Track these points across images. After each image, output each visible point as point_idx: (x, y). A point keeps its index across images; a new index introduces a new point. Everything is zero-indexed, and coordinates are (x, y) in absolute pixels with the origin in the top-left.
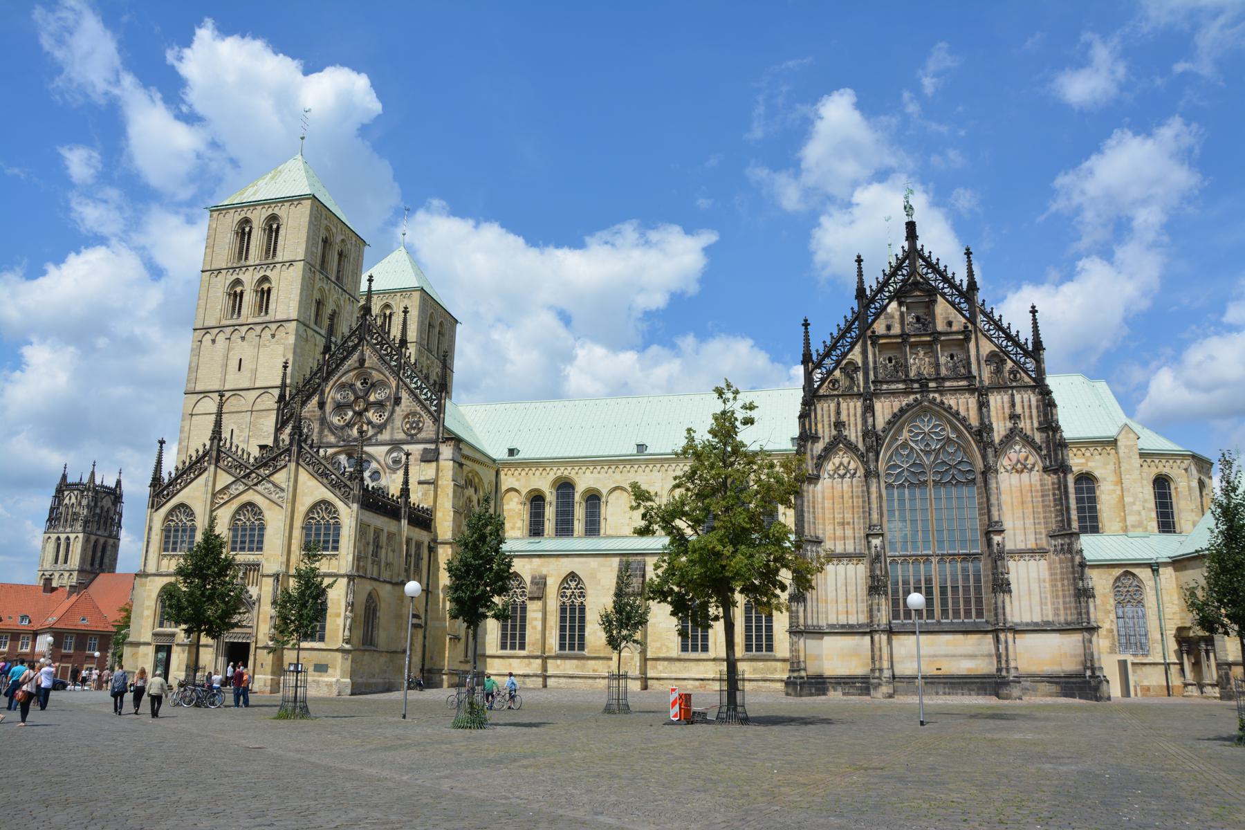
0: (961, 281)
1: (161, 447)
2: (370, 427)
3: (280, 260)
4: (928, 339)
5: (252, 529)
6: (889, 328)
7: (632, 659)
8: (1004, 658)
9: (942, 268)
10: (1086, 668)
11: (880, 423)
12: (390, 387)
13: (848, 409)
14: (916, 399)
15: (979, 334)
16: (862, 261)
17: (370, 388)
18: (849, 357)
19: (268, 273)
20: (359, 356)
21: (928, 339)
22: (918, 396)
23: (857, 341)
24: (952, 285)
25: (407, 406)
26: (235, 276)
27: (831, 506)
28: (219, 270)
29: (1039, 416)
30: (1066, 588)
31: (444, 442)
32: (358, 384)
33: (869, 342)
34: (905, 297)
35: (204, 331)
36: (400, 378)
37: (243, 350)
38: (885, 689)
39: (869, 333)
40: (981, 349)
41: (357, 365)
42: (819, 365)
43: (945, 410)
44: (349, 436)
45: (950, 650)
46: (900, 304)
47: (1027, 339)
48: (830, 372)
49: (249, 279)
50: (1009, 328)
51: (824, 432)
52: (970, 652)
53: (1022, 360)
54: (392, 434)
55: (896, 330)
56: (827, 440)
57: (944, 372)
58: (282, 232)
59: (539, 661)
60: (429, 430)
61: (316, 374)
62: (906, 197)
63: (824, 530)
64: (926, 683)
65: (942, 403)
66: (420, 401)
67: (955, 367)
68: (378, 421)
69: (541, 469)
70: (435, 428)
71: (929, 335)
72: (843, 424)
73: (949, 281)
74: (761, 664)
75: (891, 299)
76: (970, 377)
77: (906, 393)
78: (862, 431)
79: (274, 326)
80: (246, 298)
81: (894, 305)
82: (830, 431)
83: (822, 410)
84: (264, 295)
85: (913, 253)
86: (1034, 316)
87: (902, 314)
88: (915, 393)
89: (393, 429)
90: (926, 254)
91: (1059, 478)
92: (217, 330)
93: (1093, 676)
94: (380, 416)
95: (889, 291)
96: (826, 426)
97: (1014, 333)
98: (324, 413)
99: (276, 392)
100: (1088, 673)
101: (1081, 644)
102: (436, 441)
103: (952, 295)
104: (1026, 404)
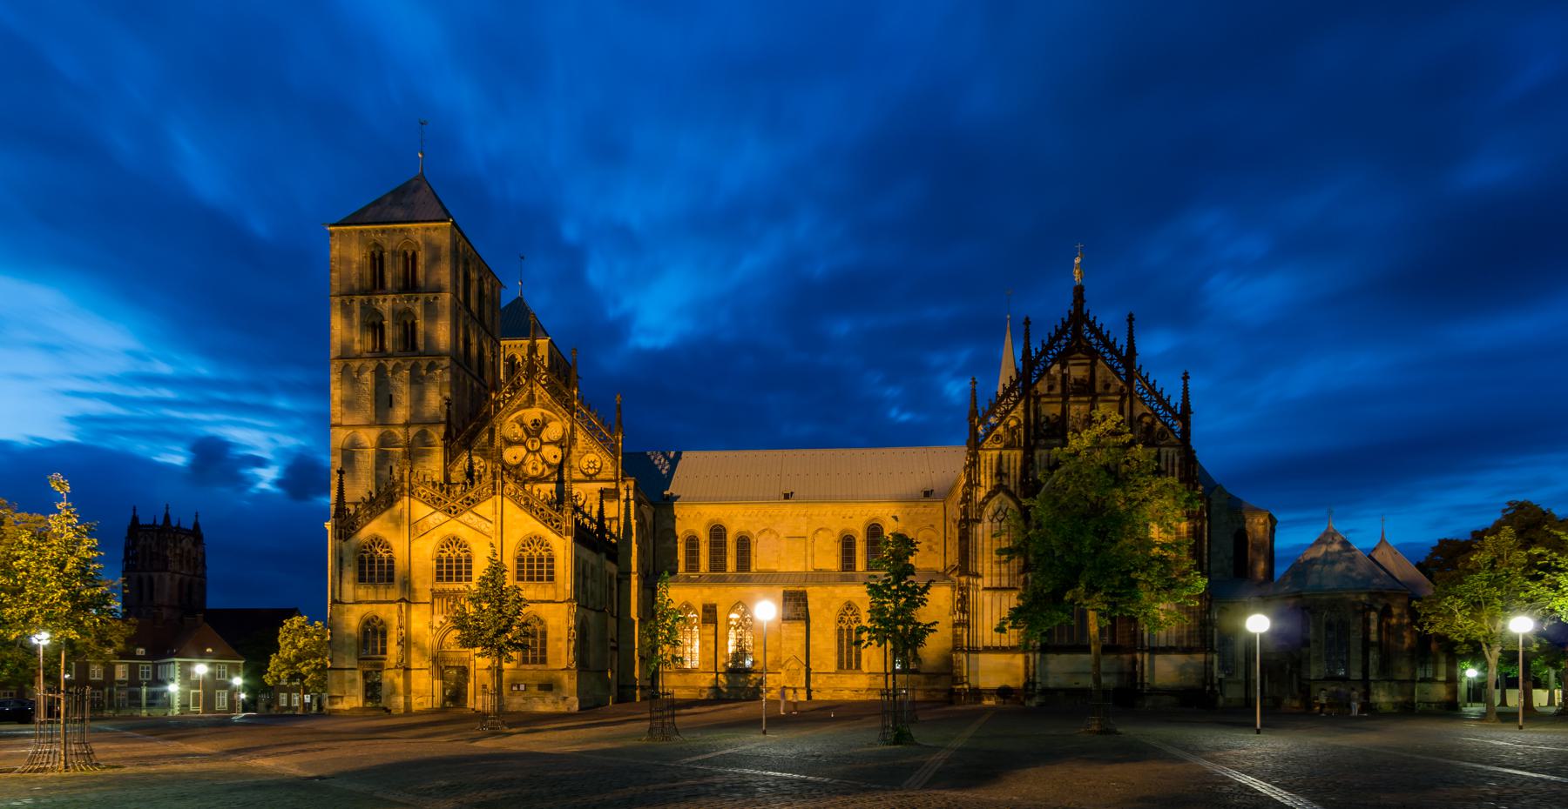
0: (1122, 346)
2: (545, 465)
5: (459, 561)
6: (1051, 388)
9: (1105, 334)
17: (541, 429)
20: (528, 397)
23: (1020, 400)
25: (584, 448)
27: (989, 547)
29: (1180, 473)
33: (1032, 401)
39: (1032, 391)
40: (1135, 411)
41: (527, 405)
42: (983, 421)
44: (526, 475)
46: (1063, 367)
47: (1177, 404)
48: (994, 427)
50: (1161, 392)
51: (986, 482)
53: (1170, 422)
55: (1058, 390)
56: (988, 489)
63: (983, 567)
70: (613, 469)
72: (1005, 474)
73: (1111, 347)
75: (1054, 361)
81: (1057, 367)
82: (992, 481)
83: (985, 462)
87: (1065, 377)
91: (1195, 527)
94: (555, 457)
95: (1053, 354)
96: (988, 477)
97: (1165, 397)
103: (1111, 359)
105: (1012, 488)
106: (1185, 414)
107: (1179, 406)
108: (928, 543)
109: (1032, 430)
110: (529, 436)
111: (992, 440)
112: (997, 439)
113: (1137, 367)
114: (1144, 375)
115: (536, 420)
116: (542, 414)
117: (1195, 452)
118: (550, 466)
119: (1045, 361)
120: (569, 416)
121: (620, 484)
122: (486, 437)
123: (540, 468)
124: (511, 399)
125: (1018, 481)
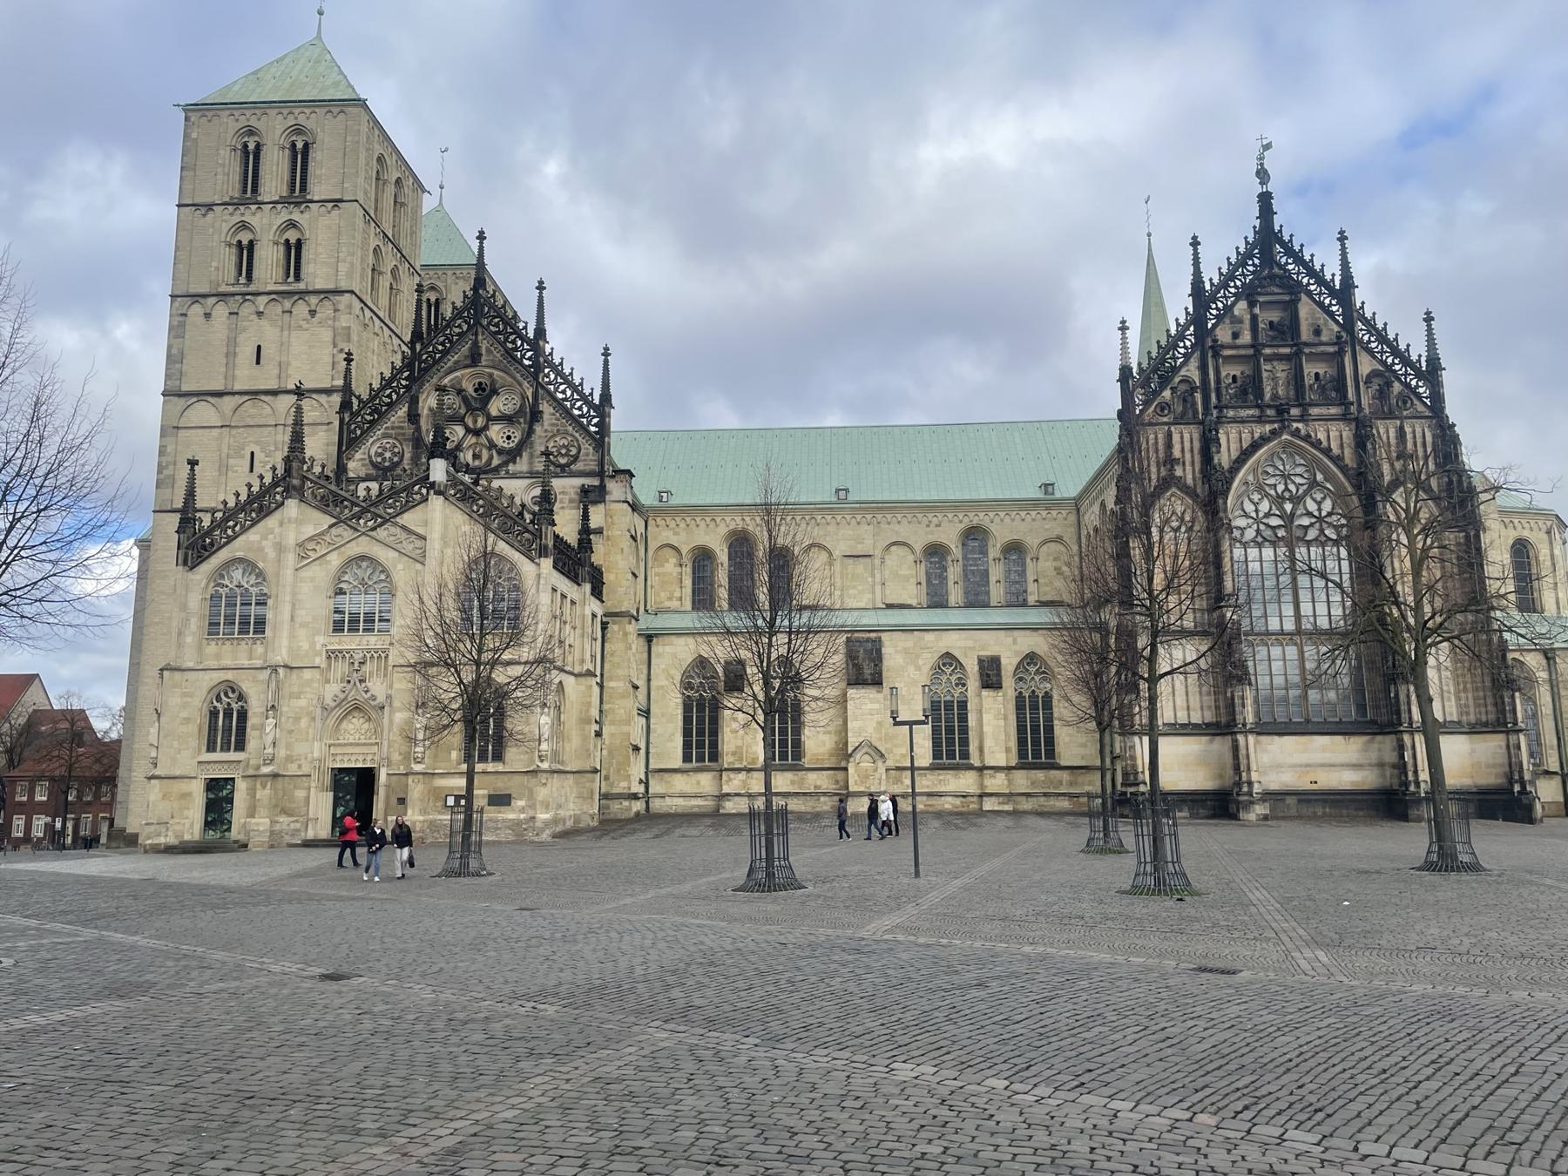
0: (1333, 275)
1: (192, 470)
3: (316, 198)
4: (1287, 350)
6: (1235, 335)
7: (876, 770)
8: (1410, 767)
10: (1511, 782)
11: (1226, 464)
12: (523, 397)
13: (1182, 443)
14: (1273, 432)
15: (1358, 348)
16: (1199, 244)
18: (1183, 372)
19: (296, 216)
20: (471, 349)
21: (1287, 350)
22: (1276, 426)
23: (1193, 353)
24: (1321, 281)
25: (553, 425)
26: (237, 218)
28: (210, 207)
30: (1479, 679)
31: (613, 477)
32: (471, 390)
33: (1210, 354)
34: (1260, 294)
35: (189, 301)
36: (538, 383)
37: (267, 332)
38: (1260, 809)
41: (468, 362)
43: (1312, 445)
45: (1328, 757)
46: (1252, 305)
47: (1420, 356)
48: (1156, 393)
49: (266, 224)
52: (1354, 761)
54: (531, 463)
55: (1246, 338)
57: (1310, 396)
58: (316, 155)
59: (742, 775)
60: (589, 459)
61: (401, 371)
62: (1261, 158)
64: (1299, 801)
65: (1307, 439)
66: (572, 417)
67: (1323, 388)
68: (505, 445)
69: (708, 519)
71: (1291, 346)
74: (1040, 775)
76: (1343, 401)
77: (1260, 420)
78: (1202, 471)
79: (313, 300)
80: (259, 253)
81: (1242, 305)
82: (1159, 471)
84: (294, 252)
85: (1267, 237)
86: (1429, 326)
87: (1254, 318)
88: (1273, 422)
89: (531, 456)
90: (1286, 238)
91: (1467, 537)
92: (212, 300)
93: (1523, 791)
94: (509, 438)
97: (1402, 347)
98: (418, 429)
99: (336, 399)
100: (1517, 788)
101: (1504, 750)
102: (601, 474)
104: (1419, 441)
105: (1189, 481)
106: (1432, 372)
107: (1423, 359)
108: (1055, 564)
109: (1213, 396)
110: (470, 409)
111: (1155, 411)
112: (1162, 409)
113: (1358, 305)
114: (1368, 315)
115: (480, 384)
116: (491, 375)
117: (1454, 425)
118: (500, 452)
119: (1225, 296)
120: (531, 379)
121: (606, 479)
122: (405, 409)
123: (485, 455)
124: (445, 353)
125: (1197, 469)
